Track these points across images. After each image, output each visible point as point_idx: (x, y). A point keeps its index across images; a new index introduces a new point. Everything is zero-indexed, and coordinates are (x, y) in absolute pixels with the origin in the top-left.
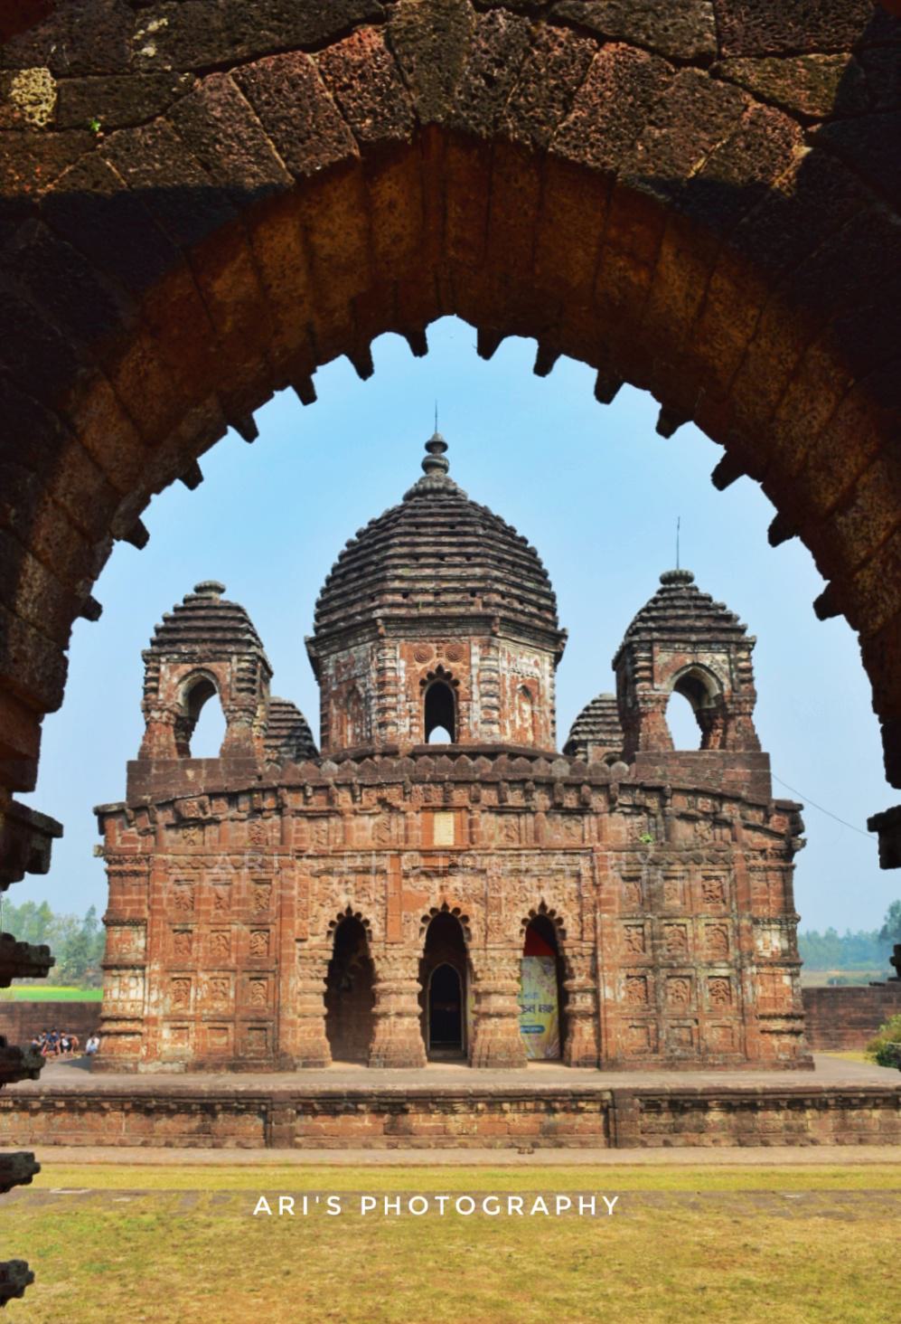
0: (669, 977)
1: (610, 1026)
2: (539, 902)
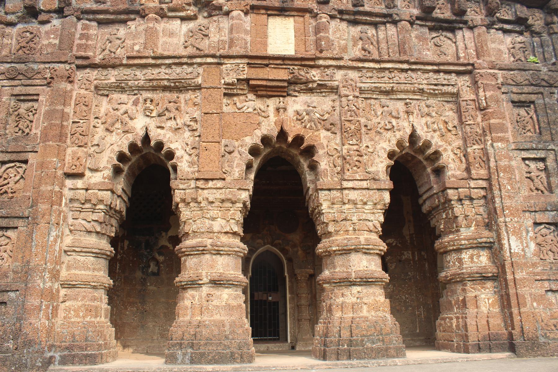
1: (523, 291)
2: (409, 131)
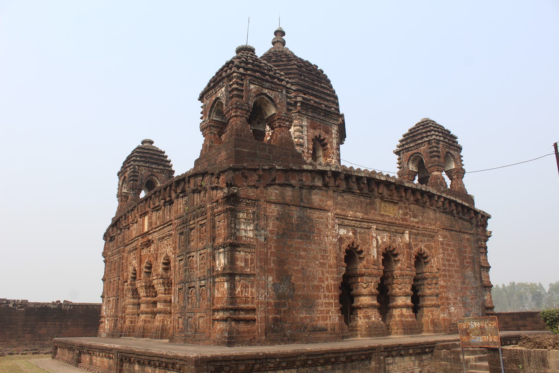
0: (190, 288)
